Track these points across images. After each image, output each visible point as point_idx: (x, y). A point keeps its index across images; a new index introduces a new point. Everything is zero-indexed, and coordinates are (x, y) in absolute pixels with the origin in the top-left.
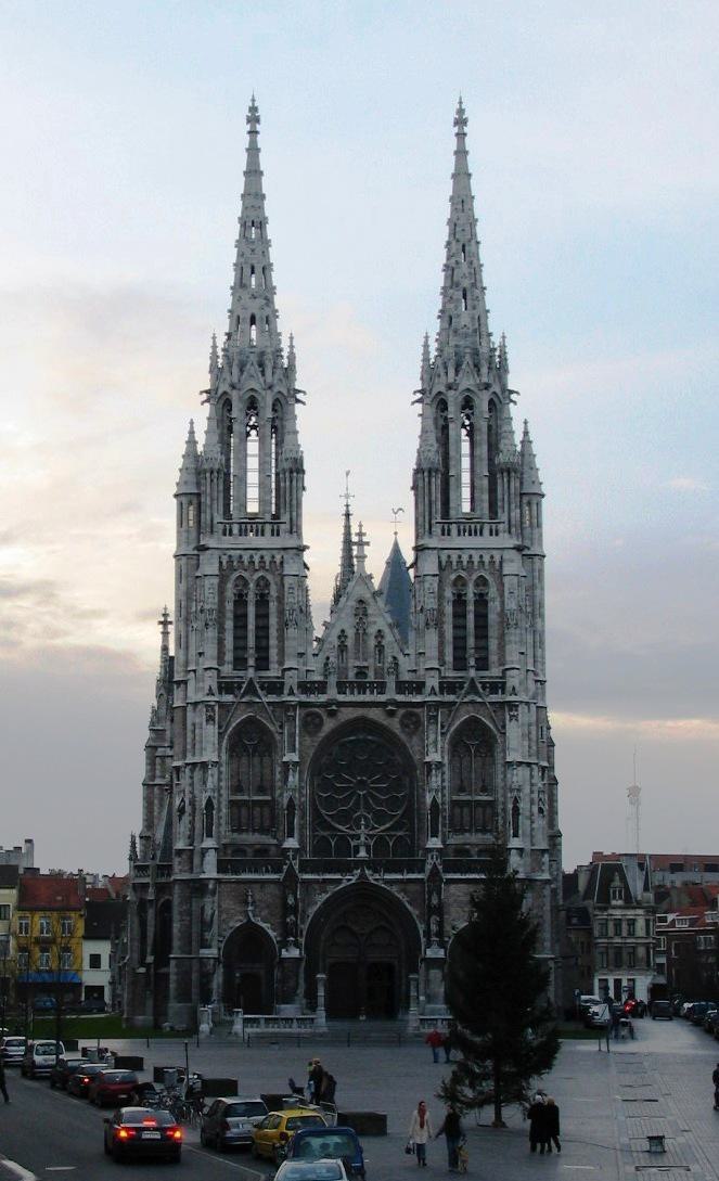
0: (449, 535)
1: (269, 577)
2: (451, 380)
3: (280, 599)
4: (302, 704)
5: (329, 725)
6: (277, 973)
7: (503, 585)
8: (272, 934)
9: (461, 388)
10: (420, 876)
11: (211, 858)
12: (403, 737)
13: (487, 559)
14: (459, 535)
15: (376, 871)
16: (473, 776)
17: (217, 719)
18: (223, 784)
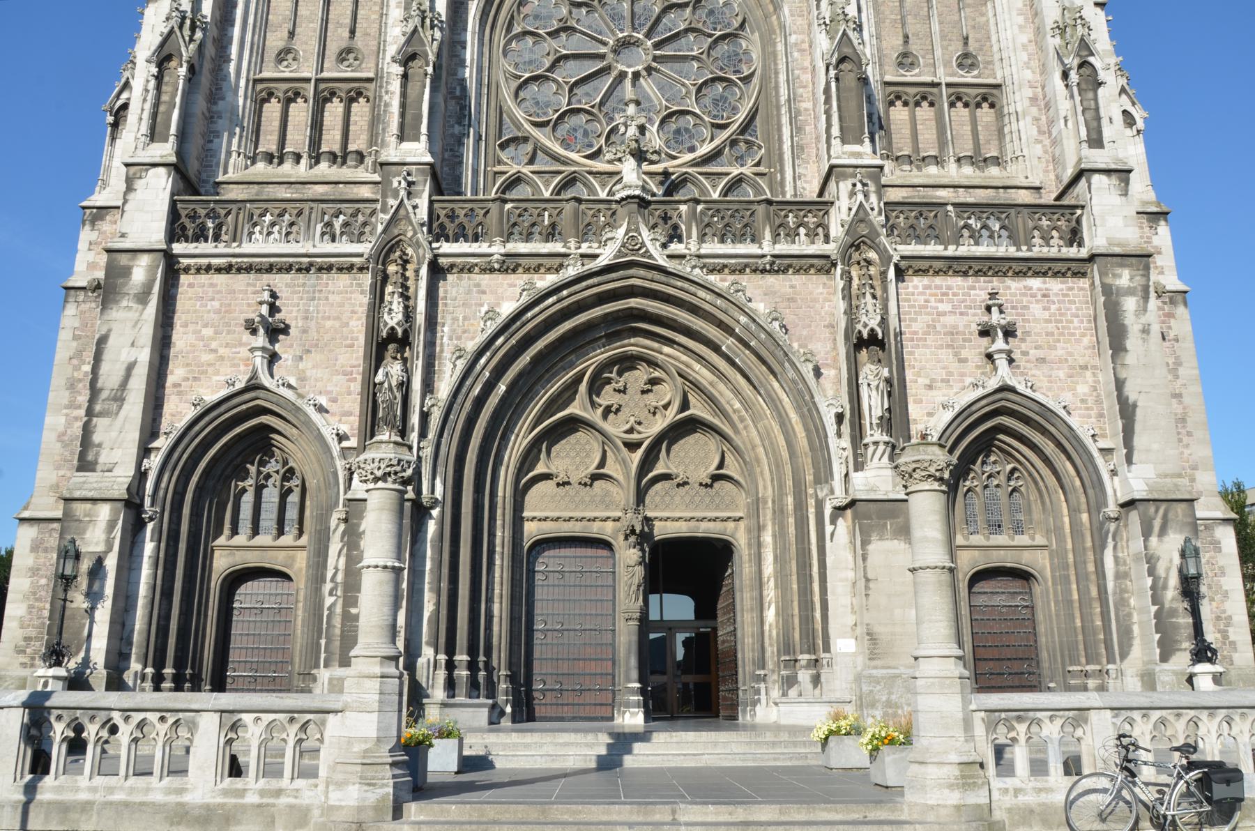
8: (327, 427)
10: (812, 250)
15: (675, 235)
16: (936, 27)
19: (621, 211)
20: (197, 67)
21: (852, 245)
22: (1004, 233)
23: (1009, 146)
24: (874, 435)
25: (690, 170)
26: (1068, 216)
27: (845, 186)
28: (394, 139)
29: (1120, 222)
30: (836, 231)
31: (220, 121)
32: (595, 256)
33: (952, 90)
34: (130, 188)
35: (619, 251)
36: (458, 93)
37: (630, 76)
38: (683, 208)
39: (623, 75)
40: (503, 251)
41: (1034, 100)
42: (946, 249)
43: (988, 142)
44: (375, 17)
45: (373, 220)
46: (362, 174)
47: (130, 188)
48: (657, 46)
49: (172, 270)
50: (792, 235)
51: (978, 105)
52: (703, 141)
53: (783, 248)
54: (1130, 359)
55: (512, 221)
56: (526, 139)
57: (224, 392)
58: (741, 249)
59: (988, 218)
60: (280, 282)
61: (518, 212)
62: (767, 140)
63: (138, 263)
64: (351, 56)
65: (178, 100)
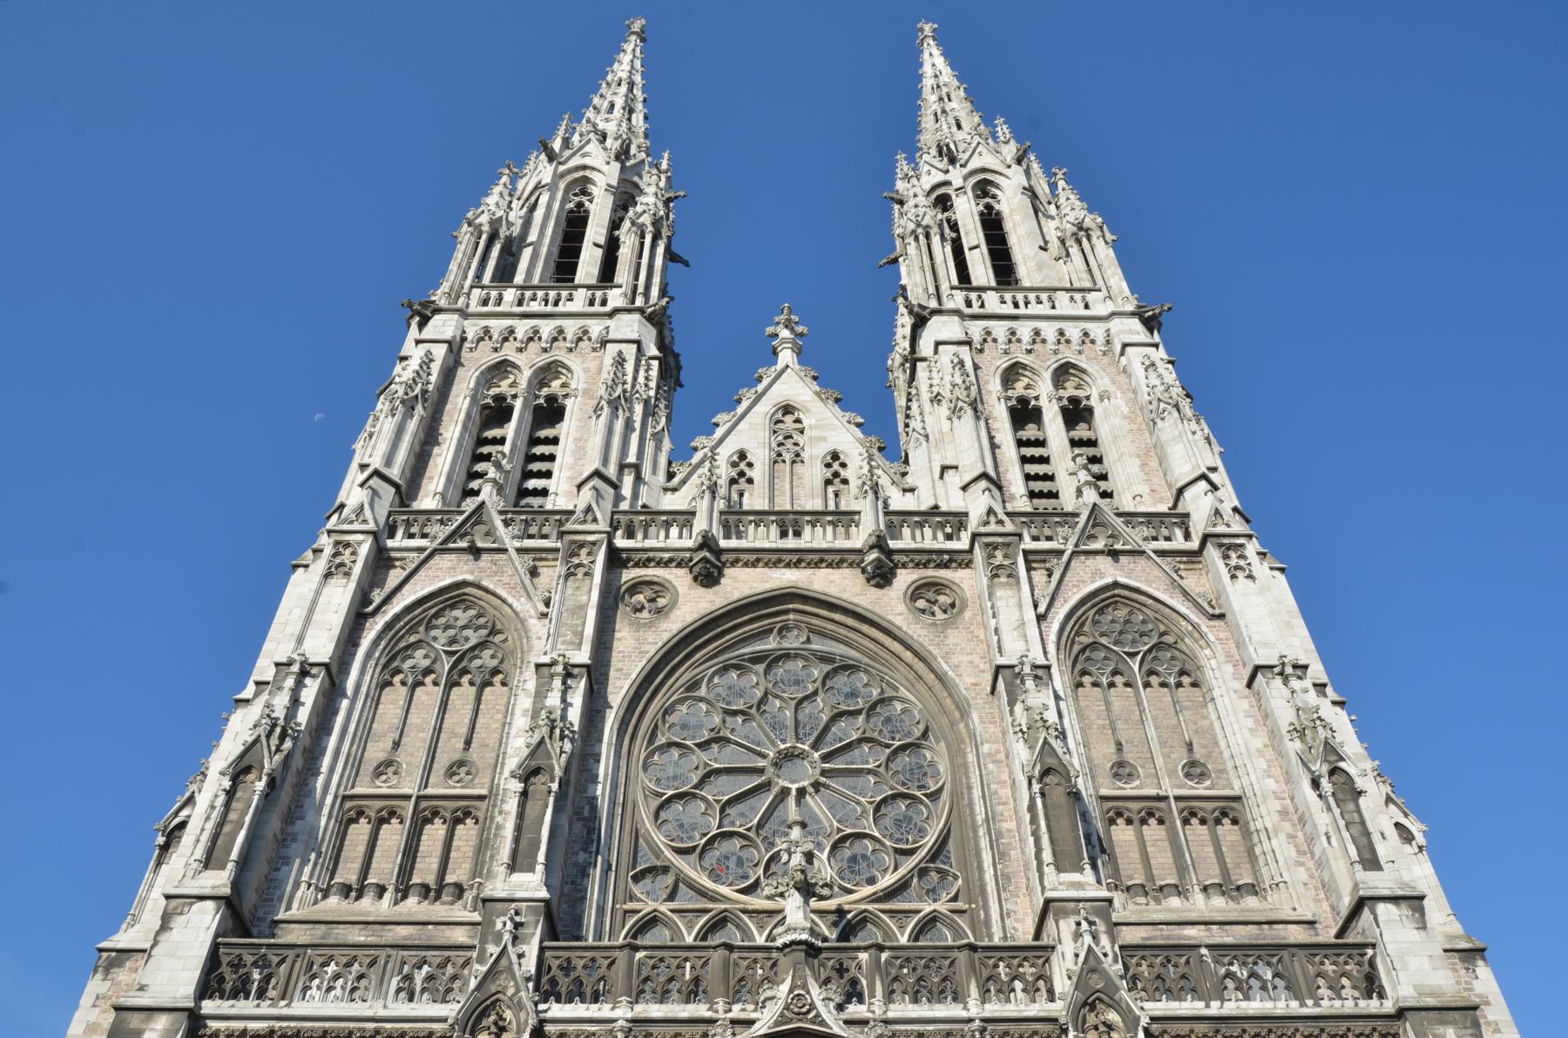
1: (571, 361)
5: (693, 603)
9: (975, 163)
10: (1033, 1010)
12: (917, 631)
15: (853, 993)
16: (1152, 732)
17: (357, 569)
19: (784, 961)
20: (278, 781)
21: (1085, 1004)
22: (1280, 983)
23: (1264, 870)
25: (870, 907)
26: (1357, 958)
27: (1067, 926)
28: (503, 869)
29: (1426, 965)
30: (1062, 985)
31: (294, 845)
32: (751, 1023)
33: (1183, 804)
34: (165, 926)
35: (782, 1015)
36: (586, 813)
37: (794, 793)
38: (863, 956)
39: (785, 792)
40: (629, 1015)
41: (1283, 813)
42: (1208, 1006)
43: (1238, 866)
44: (497, 725)
45: (466, 972)
46: (460, 912)
47: (165, 926)
48: (826, 758)
50: (1006, 992)
51: (1218, 822)
52: (885, 870)
55: (644, 974)
56: (665, 870)
59: (1255, 963)
61: (651, 962)
62: (965, 868)
63: (152, 1025)
64: (463, 770)
65: (248, 819)
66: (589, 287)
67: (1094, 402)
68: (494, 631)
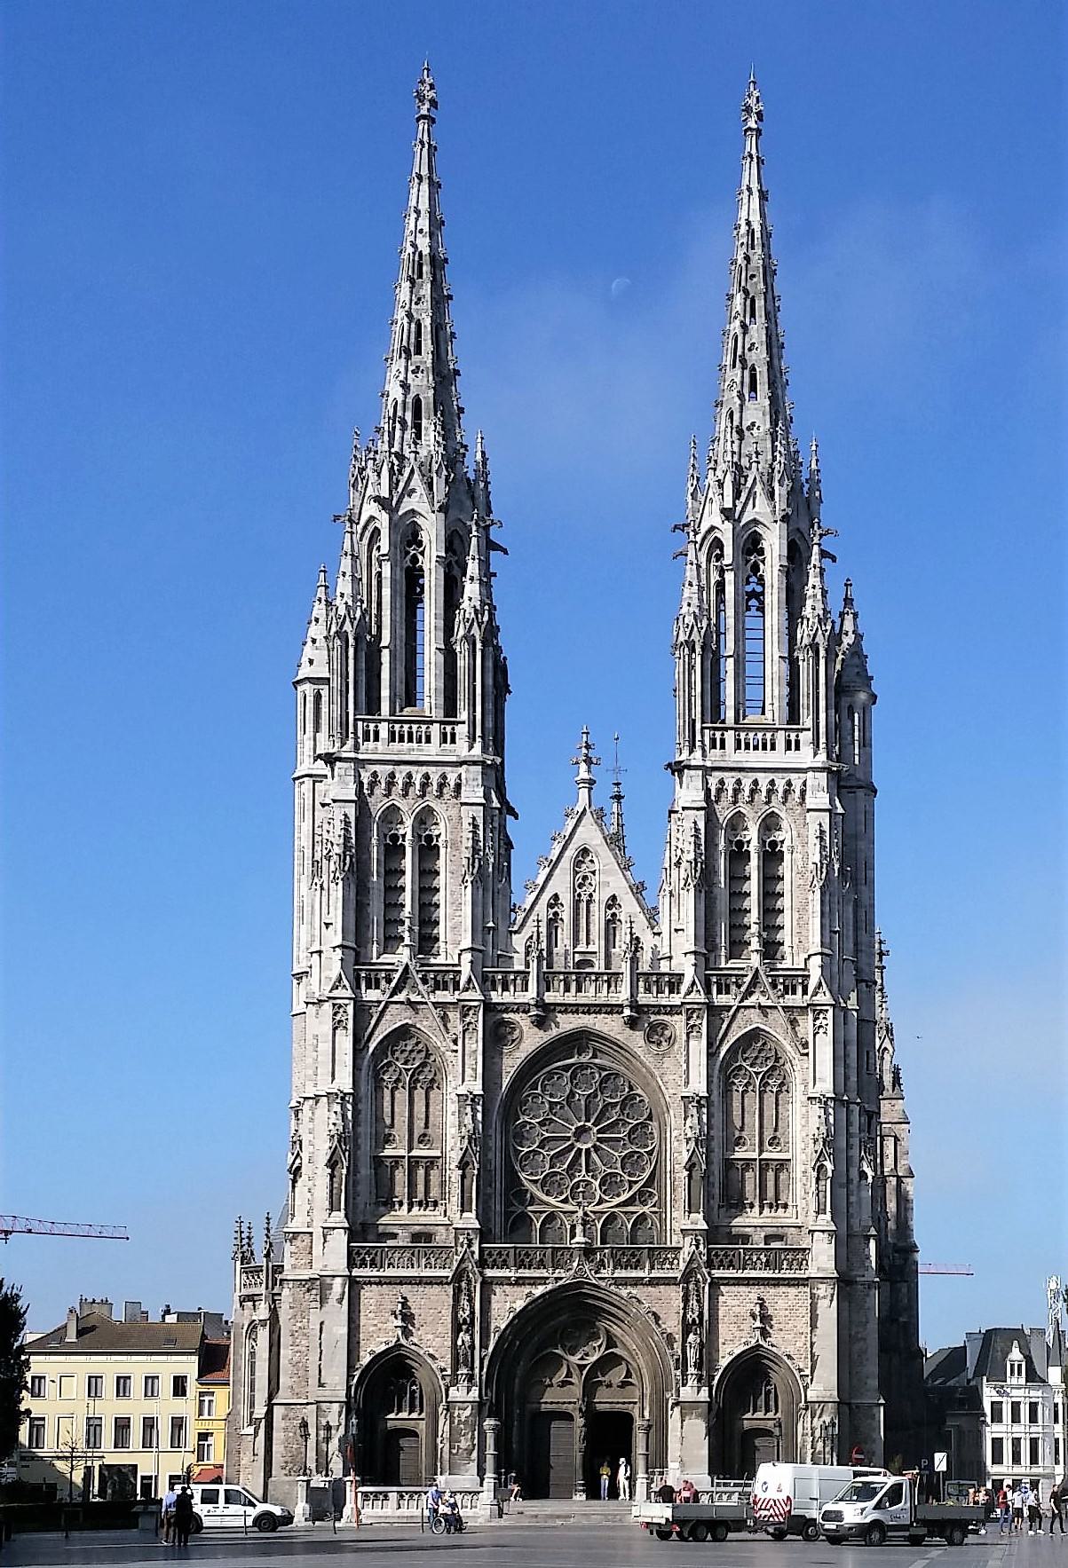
0: (723, 747)
2: (728, 504)
3: (455, 845)
4: (489, 1007)
5: (531, 1039)
6: (443, 1427)
7: (806, 824)
11: (340, 1240)
12: (648, 1060)
13: (780, 785)
14: (739, 747)
15: (602, 1264)
17: (350, 1026)
18: (360, 1129)
24: (691, 1370)
27: (688, 1239)
48: (599, 1132)
49: (354, 1285)
53: (655, 1274)
54: (818, 1331)
57: (383, 1347)
58: (634, 1274)
60: (405, 1289)
66: (441, 723)
67: (784, 849)
68: (428, 1055)
